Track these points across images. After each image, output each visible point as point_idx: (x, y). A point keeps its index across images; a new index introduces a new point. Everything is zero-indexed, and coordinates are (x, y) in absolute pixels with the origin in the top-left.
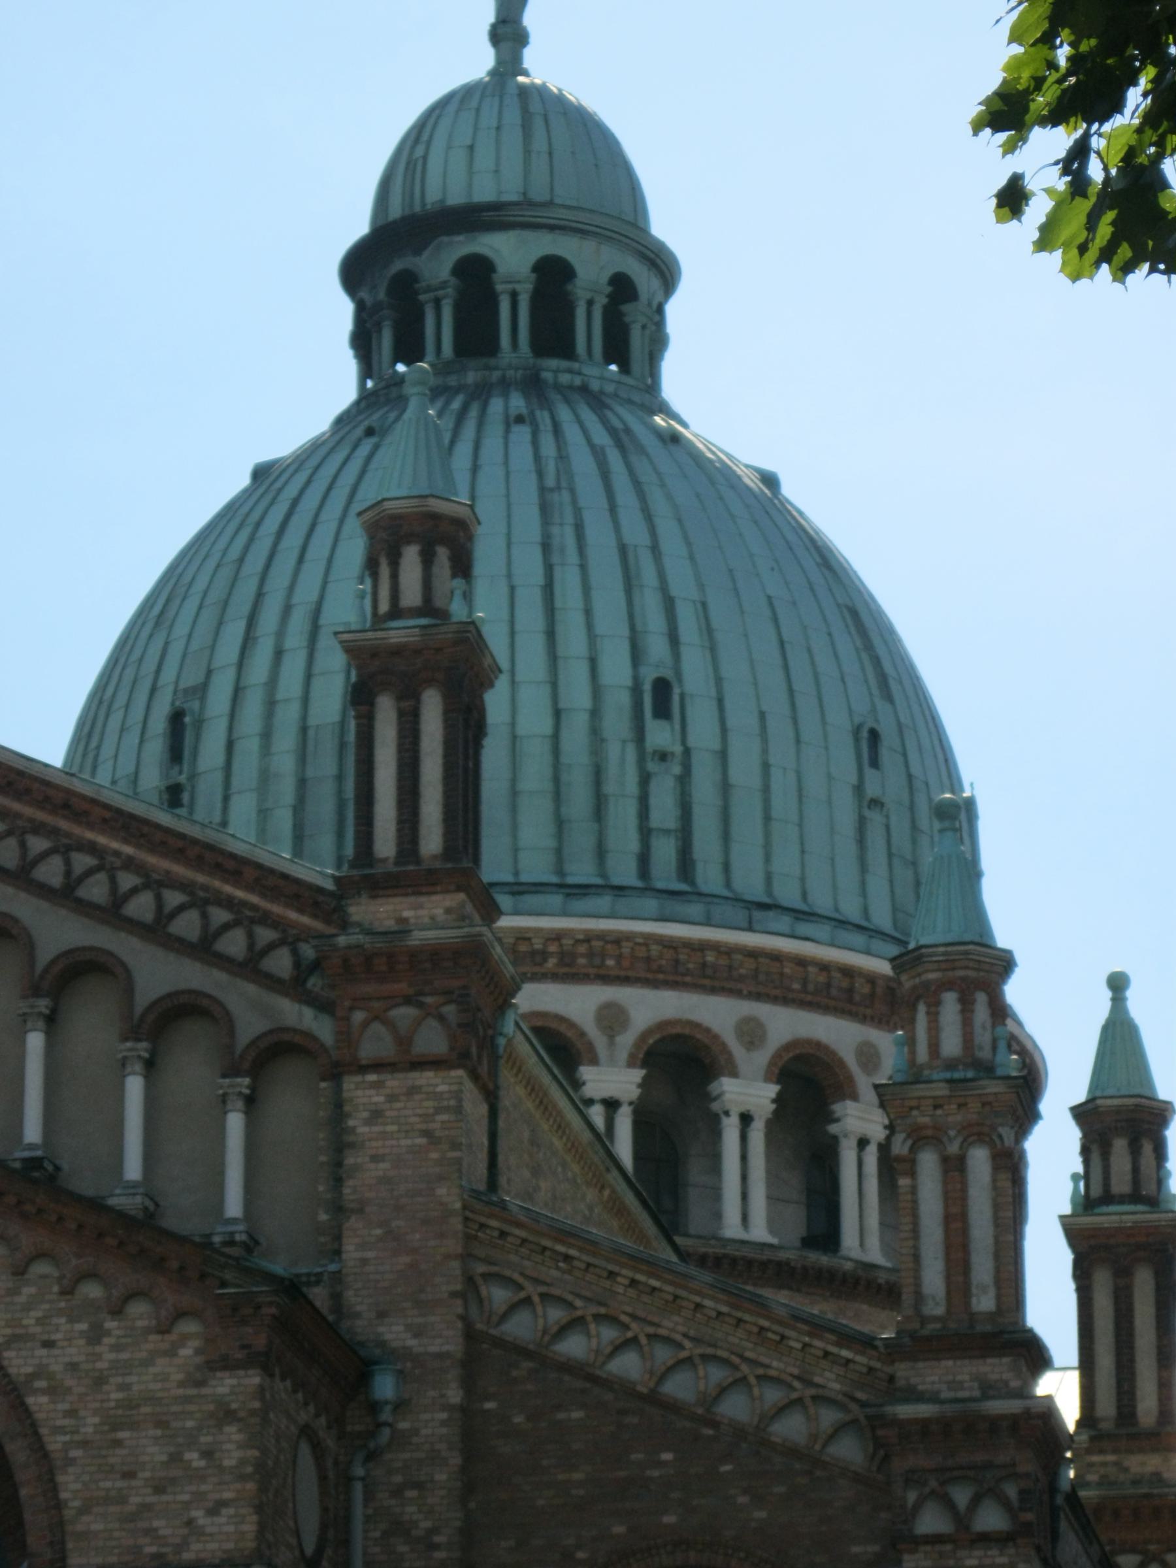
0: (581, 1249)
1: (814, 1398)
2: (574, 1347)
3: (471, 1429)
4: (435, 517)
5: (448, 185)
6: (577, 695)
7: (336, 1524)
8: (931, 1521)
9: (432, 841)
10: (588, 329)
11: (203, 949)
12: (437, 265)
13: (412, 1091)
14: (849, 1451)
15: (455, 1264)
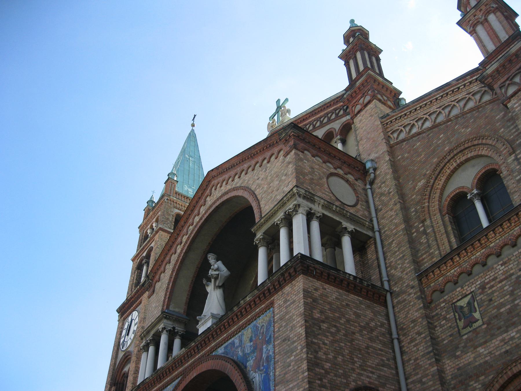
0: (407, 110)
1: (473, 95)
4: (352, 31)
7: (362, 199)
13: (366, 112)
15: (382, 134)
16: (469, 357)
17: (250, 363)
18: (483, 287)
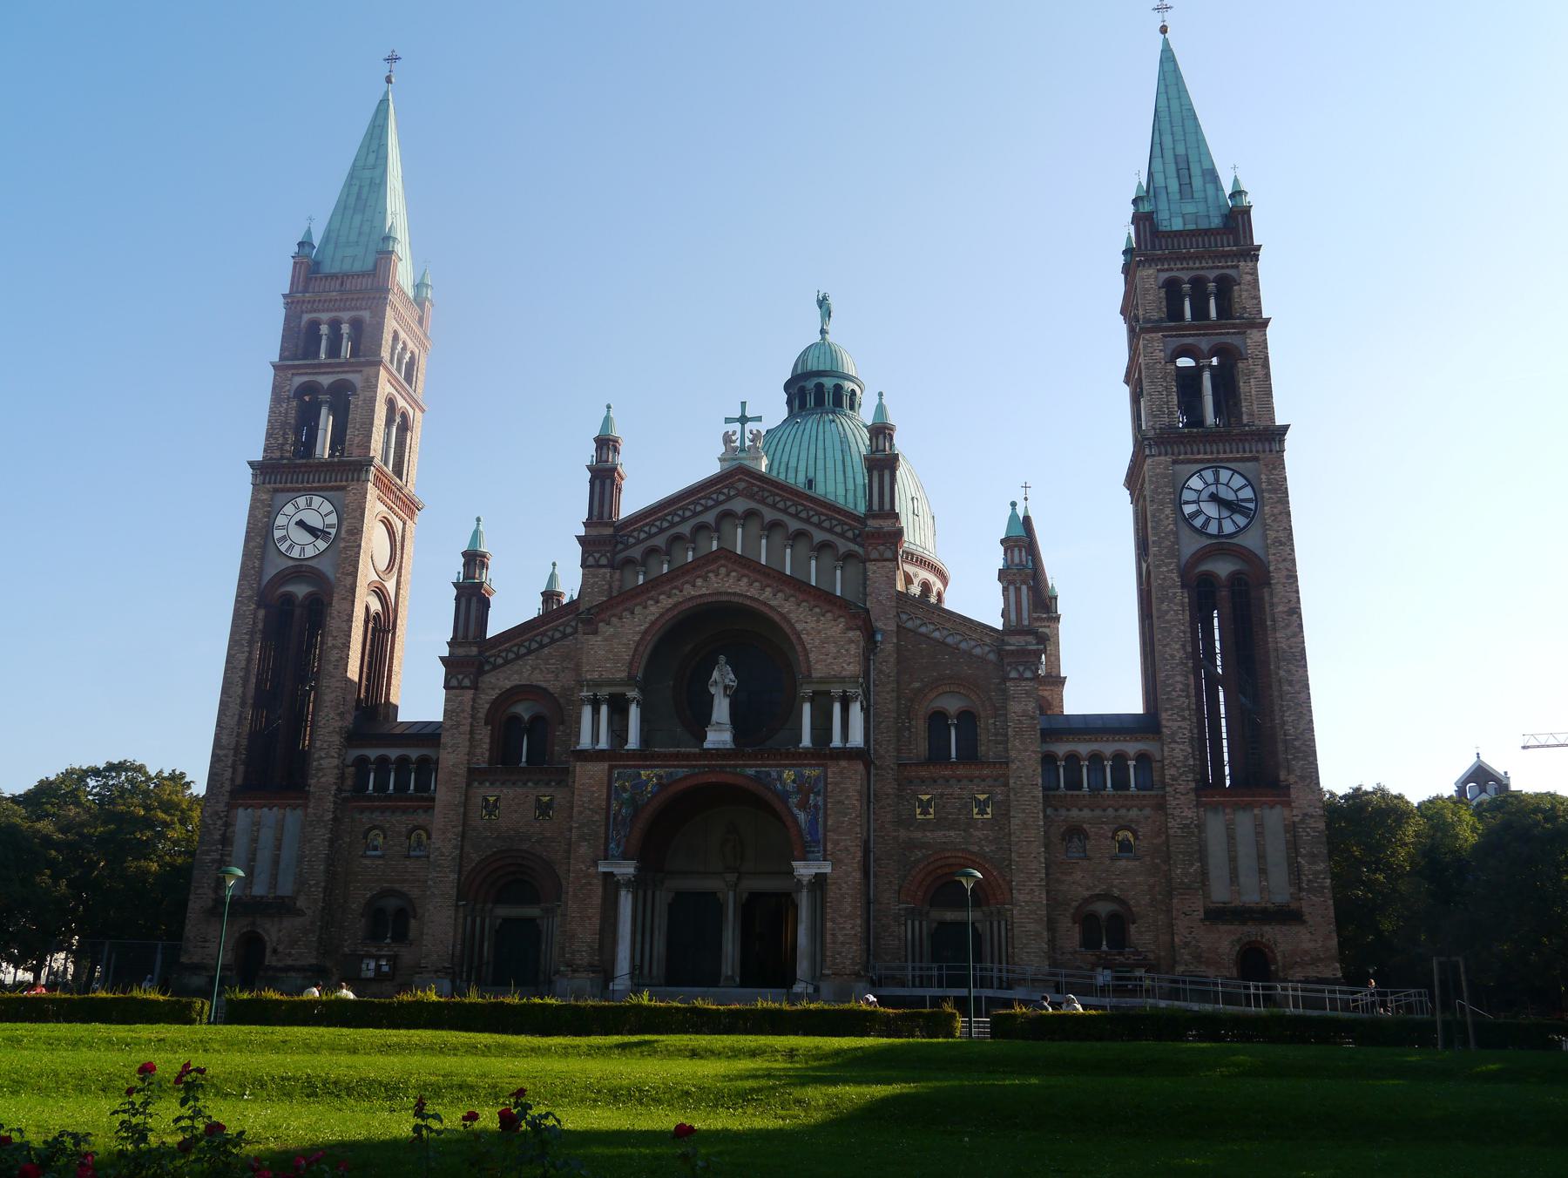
2: (923, 630)
3: (899, 649)
5: (812, 365)
6: (851, 486)
8: (1013, 675)
9: (887, 506)
10: (846, 401)
11: (831, 530)
12: (810, 384)
14: (992, 657)
16: (918, 835)
17: (794, 800)
18: (942, 795)
